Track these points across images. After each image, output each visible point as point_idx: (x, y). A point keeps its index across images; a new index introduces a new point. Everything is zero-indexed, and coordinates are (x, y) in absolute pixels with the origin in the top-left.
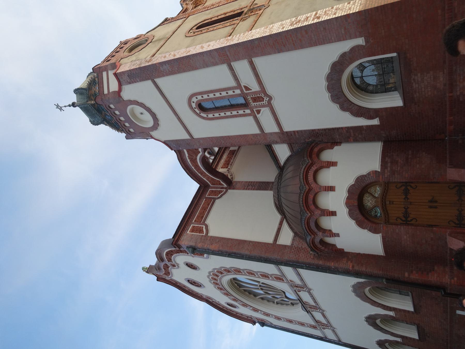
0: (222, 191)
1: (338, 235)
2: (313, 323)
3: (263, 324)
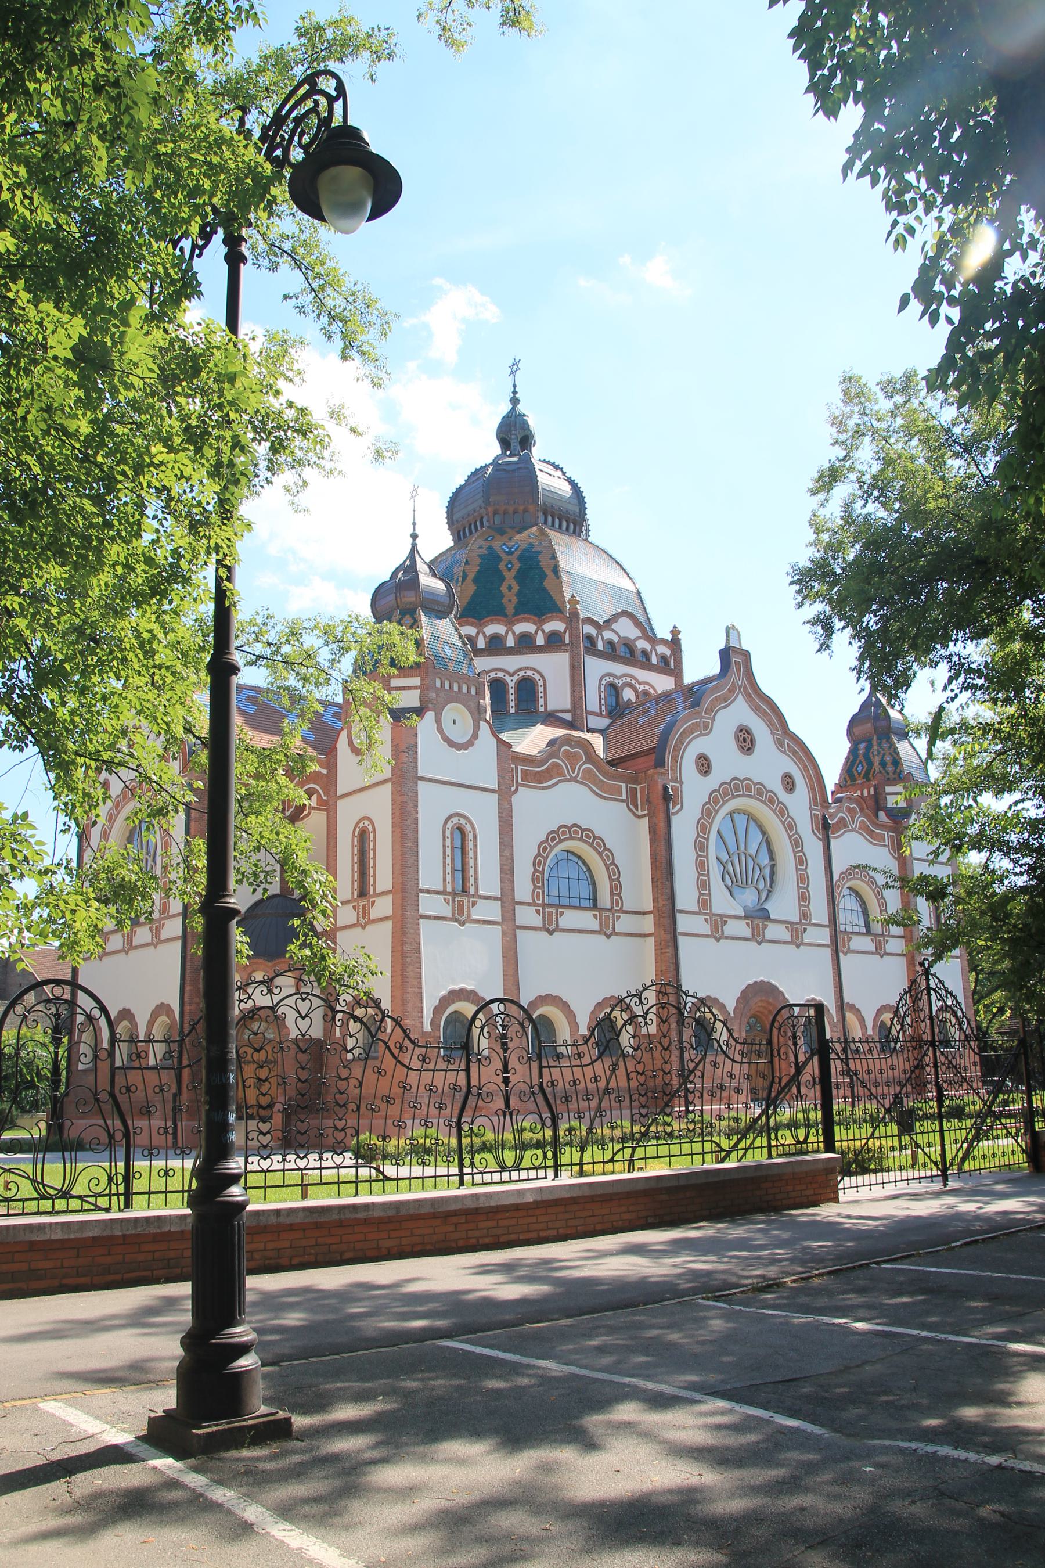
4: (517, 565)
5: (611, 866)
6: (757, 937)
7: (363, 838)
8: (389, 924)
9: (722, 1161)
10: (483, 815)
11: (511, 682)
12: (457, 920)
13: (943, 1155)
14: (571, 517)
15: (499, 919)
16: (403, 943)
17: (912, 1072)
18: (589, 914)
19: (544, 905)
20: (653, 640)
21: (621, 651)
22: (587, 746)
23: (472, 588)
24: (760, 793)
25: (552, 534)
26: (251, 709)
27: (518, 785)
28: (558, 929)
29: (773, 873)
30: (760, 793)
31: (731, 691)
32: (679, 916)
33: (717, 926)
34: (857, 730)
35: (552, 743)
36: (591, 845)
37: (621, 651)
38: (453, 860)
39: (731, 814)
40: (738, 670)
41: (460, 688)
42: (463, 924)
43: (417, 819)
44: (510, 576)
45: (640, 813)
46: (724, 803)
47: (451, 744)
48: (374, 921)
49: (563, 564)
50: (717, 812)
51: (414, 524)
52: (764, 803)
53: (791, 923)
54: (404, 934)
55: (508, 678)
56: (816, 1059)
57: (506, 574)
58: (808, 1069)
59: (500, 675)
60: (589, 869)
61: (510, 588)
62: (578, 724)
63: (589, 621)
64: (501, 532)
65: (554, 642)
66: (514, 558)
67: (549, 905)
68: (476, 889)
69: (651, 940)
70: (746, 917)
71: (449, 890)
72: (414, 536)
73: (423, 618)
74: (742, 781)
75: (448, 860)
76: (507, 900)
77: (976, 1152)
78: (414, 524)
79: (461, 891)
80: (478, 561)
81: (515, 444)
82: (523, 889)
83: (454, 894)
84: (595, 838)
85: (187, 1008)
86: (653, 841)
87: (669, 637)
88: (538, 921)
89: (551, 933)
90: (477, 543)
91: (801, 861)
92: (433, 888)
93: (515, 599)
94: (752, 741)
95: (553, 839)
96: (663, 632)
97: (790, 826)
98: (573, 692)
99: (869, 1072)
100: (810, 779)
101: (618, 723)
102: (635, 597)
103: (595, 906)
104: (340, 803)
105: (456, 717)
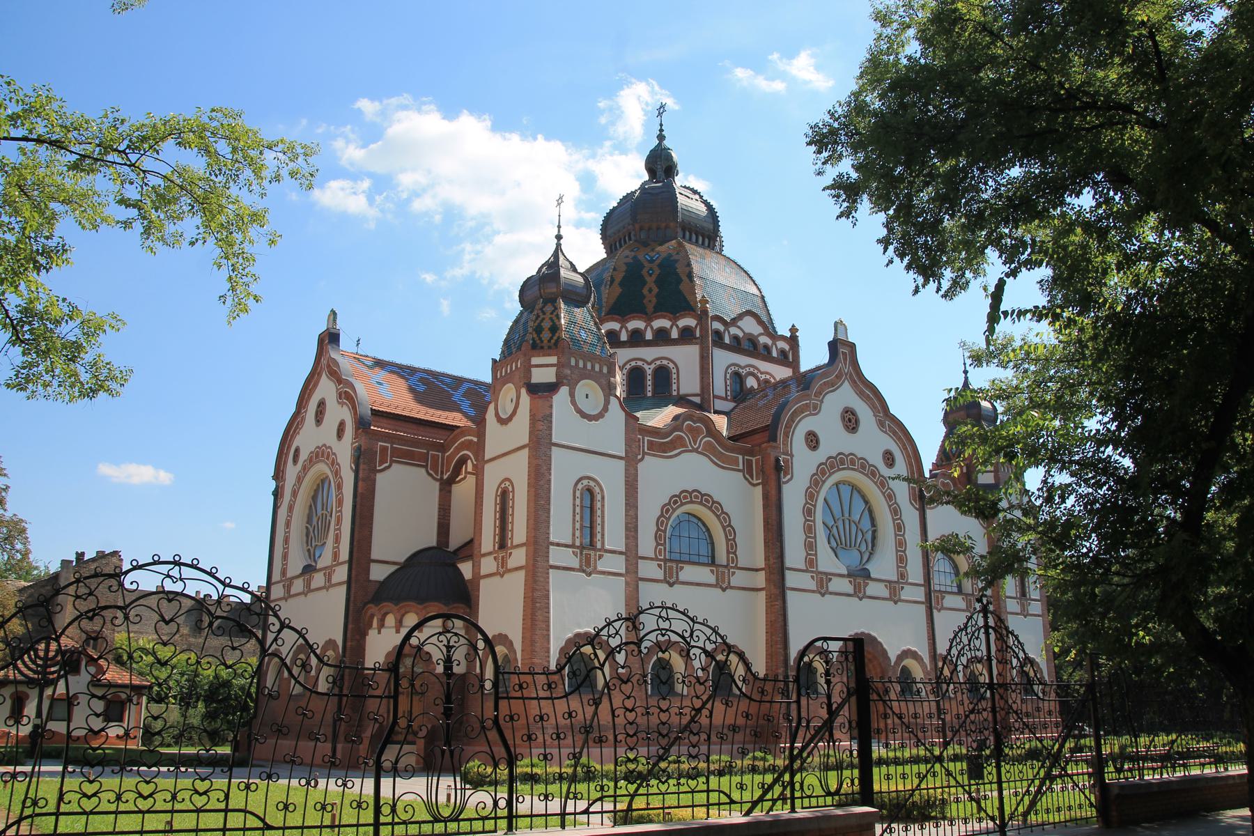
0: (437, 473)
1: (379, 632)
2: (289, 575)
3: (277, 494)
4: (657, 272)
5: (728, 528)
6: (859, 593)
7: (504, 497)
8: (521, 575)
9: (748, 813)
10: (611, 478)
11: (649, 370)
12: (584, 571)
13: (1001, 809)
14: (706, 232)
15: (623, 571)
16: (534, 590)
17: (967, 716)
18: (707, 570)
19: (665, 560)
20: (774, 336)
21: (745, 345)
22: (709, 425)
23: (618, 290)
24: (863, 467)
25: (688, 246)
26: (421, 388)
27: (644, 454)
28: (677, 582)
29: (874, 538)
30: (863, 467)
31: (839, 377)
32: (788, 574)
33: (823, 584)
34: (951, 418)
35: (676, 418)
36: (710, 509)
37: (745, 345)
38: (582, 518)
39: (837, 484)
40: (845, 359)
41: (593, 367)
42: (589, 574)
43: (549, 480)
44: (650, 281)
45: (755, 482)
46: (831, 474)
47: (584, 415)
48: (510, 571)
49: (696, 268)
50: (824, 482)
51: (559, 227)
52: (866, 475)
53: (890, 582)
54: (535, 582)
55: (646, 367)
56: (853, 699)
57: (648, 279)
58: (845, 711)
59: (640, 363)
60: (708, 530)
61: (650, 291)
62: (706, 406)
63: (718, 318)
64: (645, 244)
65: (687, 336)
66: (655, 266)
67: (671, 560)
68: (603, 544)
69: (763, 594)
70: (849, 575)
71: (578, 543)
72: (559, 237)
73: (562, 306)
74: (847, 456)
75: (578, 518)
76: (631, 554)
77: (1038, 807)
78: (559, 227)
79: (588, 546)
80: (624, 268)
81: (660, 173)
82: (646, 545)
83: (582, 547)
84: (714, 502)
85: (349, 644)
86: (766, 506)
87: (788, 334)
88: (659, 574)
89: (671, 585)
90: (624, 254)
91: (899, 527)
92: (563, 541)
93: (654, 300)
94: (857, 421)
95: (675, 502)
96: (783, 330)
97: (890, 497)
98: (702, 379)
99: (915, 716)
100: (908, 456)
101: (742, 406)
102: (759, 300)
103: (713, 563)
104: (487, 467)
105: (589, 393)
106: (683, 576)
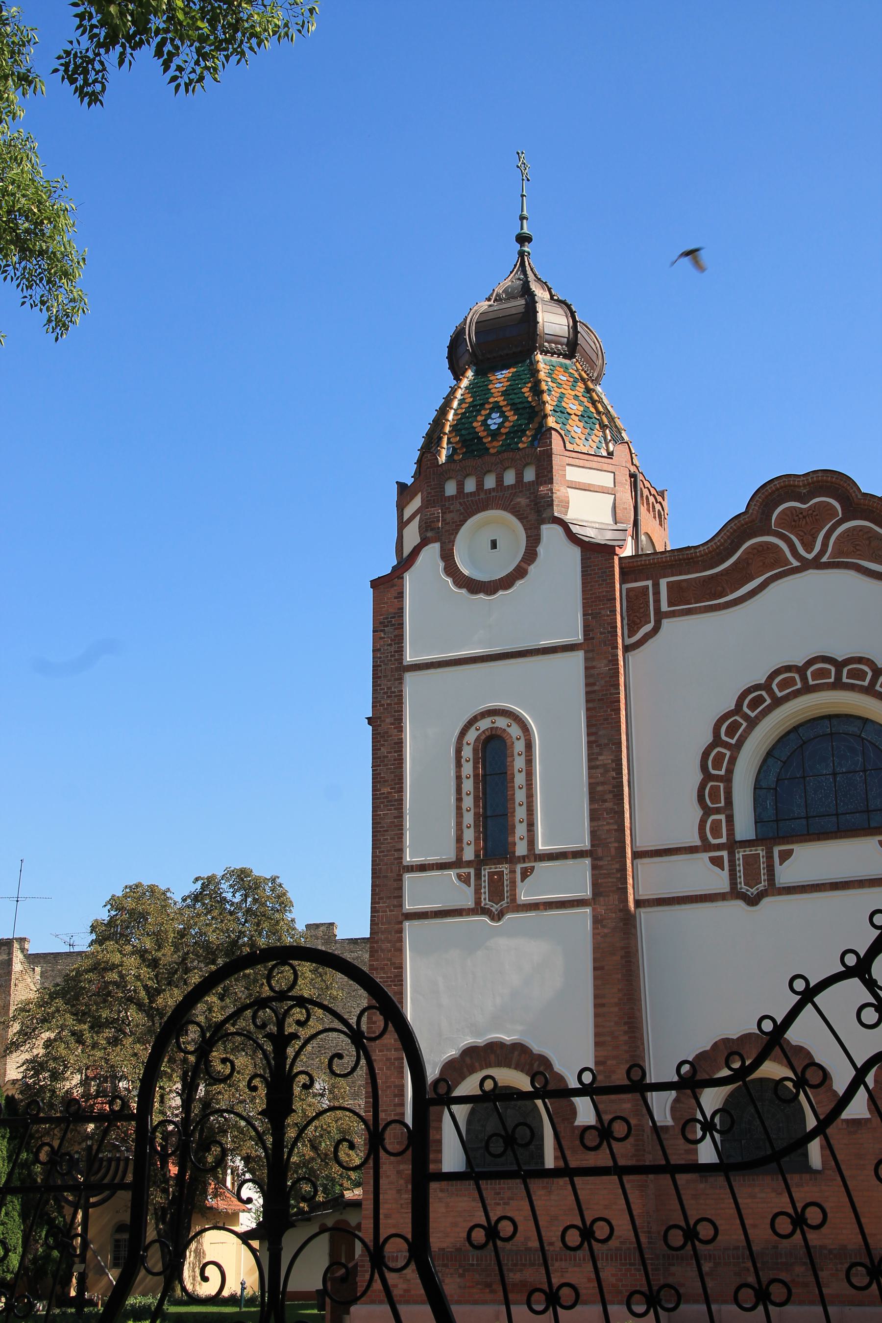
12: (485, 911)
15: (588, 893)
27: (660, 616)
28: (773, 889)
68: (532, 842)
71: (469, 854)
76: (607, 852)
83: (478, 863)
95: (756, 702)
106: (786, 874)
